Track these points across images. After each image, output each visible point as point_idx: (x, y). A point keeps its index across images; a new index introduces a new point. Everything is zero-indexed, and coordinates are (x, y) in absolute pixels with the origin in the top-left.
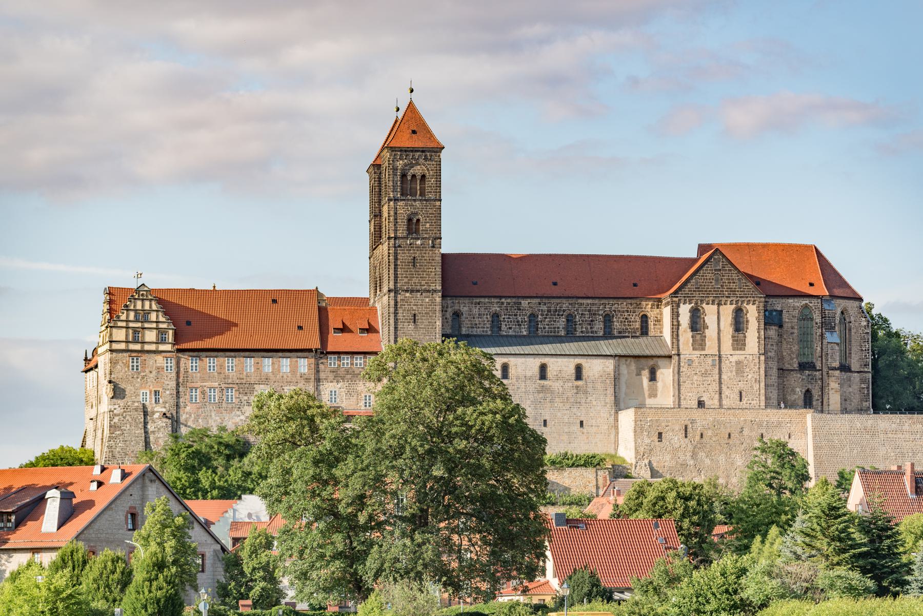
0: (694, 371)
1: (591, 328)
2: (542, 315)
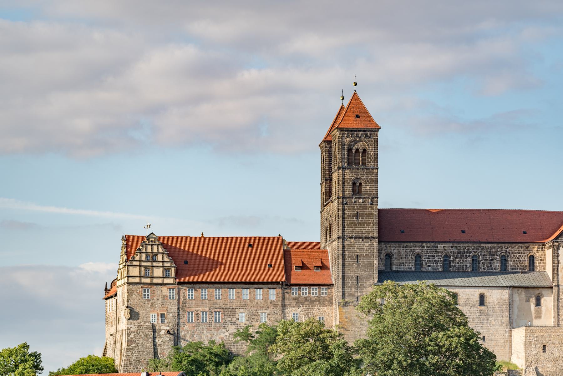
1: (491, 266)
2: (454, 256)
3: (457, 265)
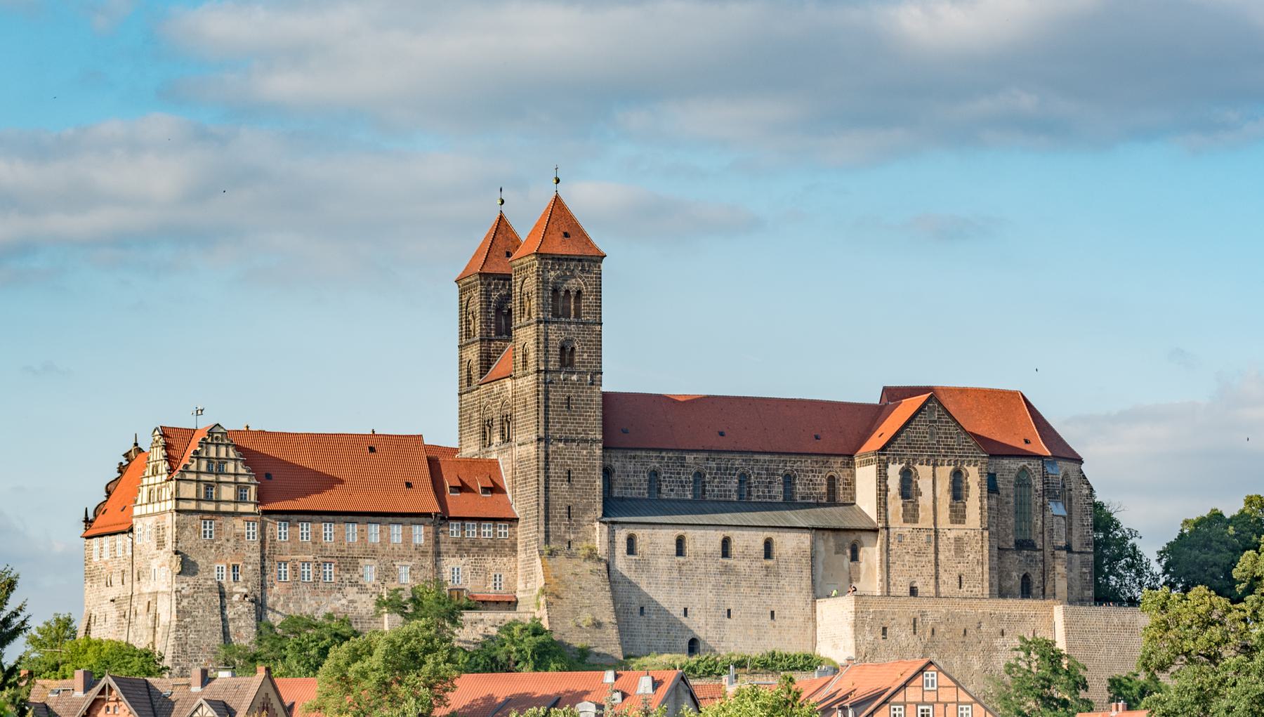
0: (905, 548)
1: (769, 492)
3: (716, 489)
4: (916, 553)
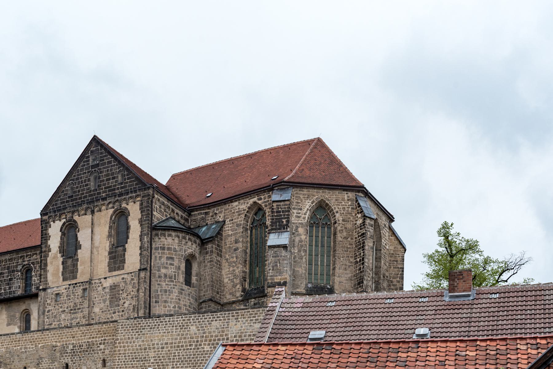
0: (61, 307)
1: (10, 288)
4: (71, 310)
